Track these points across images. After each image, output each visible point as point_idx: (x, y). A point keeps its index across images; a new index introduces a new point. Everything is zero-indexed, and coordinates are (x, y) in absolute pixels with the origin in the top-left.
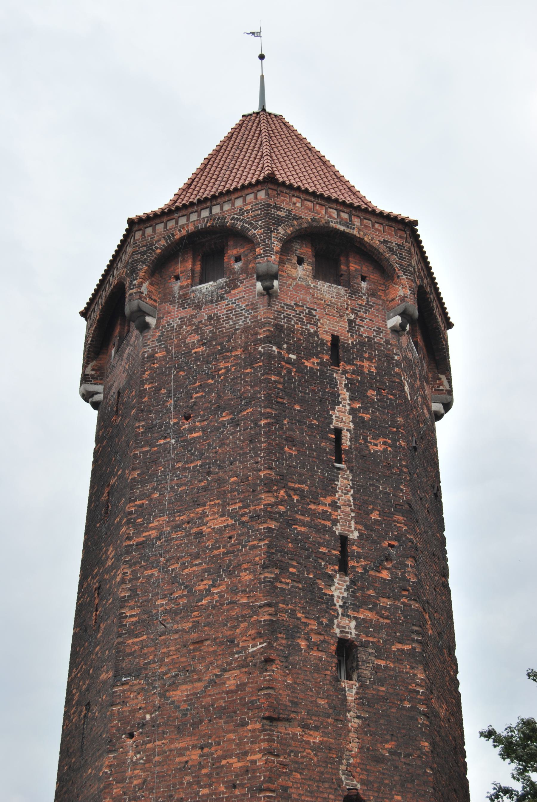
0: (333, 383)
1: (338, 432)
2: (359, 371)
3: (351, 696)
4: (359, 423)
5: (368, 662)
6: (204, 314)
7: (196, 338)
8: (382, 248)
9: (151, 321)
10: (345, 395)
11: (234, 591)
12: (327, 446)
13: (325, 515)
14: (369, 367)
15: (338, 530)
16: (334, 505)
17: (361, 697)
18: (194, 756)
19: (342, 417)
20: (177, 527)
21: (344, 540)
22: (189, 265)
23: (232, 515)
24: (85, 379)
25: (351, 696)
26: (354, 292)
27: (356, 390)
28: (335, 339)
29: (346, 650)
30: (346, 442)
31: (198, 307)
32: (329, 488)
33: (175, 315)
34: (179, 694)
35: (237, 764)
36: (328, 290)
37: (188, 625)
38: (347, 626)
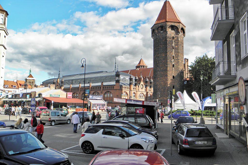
0: (173, 41)
1: (173, 46)
2: (175, 39)
3: (174, 69)
4: (175, 45)
5: (175, 66)
6: (162, 34)
7: (161, 37)
8: (177, 26)
9: (157, 35)
10: (174, 42)
11: (165, 61)
12: (172, 48)
13: (172, 54)
14: (176, 39)
15: (173, 55)
16: (173, 53)
17: (174, 69)
18: (163, 73)
19: (173, 45)
20: (161, 55)
21: (173, 56)
22: (160, 29)
23: (165, 55)
24: (152, 36)
25: (174, 69)
26: (175, 31)
27: (175, 42)
28: (173, 37)
29: (173, 65)
30: (174, 47)
31: (161, 34)
32: (172, 52)
33: (159, 34)
34: (161, 69)
35: (166, 74)
36: (173, 31)
37: (162, 63)
38: (173, 63)
